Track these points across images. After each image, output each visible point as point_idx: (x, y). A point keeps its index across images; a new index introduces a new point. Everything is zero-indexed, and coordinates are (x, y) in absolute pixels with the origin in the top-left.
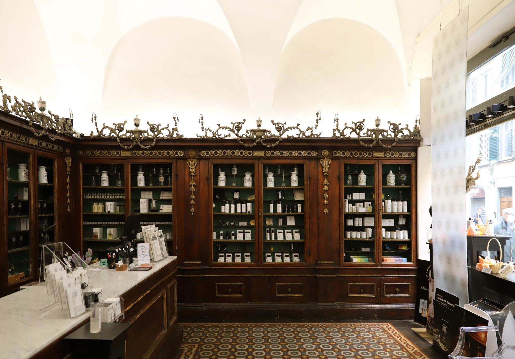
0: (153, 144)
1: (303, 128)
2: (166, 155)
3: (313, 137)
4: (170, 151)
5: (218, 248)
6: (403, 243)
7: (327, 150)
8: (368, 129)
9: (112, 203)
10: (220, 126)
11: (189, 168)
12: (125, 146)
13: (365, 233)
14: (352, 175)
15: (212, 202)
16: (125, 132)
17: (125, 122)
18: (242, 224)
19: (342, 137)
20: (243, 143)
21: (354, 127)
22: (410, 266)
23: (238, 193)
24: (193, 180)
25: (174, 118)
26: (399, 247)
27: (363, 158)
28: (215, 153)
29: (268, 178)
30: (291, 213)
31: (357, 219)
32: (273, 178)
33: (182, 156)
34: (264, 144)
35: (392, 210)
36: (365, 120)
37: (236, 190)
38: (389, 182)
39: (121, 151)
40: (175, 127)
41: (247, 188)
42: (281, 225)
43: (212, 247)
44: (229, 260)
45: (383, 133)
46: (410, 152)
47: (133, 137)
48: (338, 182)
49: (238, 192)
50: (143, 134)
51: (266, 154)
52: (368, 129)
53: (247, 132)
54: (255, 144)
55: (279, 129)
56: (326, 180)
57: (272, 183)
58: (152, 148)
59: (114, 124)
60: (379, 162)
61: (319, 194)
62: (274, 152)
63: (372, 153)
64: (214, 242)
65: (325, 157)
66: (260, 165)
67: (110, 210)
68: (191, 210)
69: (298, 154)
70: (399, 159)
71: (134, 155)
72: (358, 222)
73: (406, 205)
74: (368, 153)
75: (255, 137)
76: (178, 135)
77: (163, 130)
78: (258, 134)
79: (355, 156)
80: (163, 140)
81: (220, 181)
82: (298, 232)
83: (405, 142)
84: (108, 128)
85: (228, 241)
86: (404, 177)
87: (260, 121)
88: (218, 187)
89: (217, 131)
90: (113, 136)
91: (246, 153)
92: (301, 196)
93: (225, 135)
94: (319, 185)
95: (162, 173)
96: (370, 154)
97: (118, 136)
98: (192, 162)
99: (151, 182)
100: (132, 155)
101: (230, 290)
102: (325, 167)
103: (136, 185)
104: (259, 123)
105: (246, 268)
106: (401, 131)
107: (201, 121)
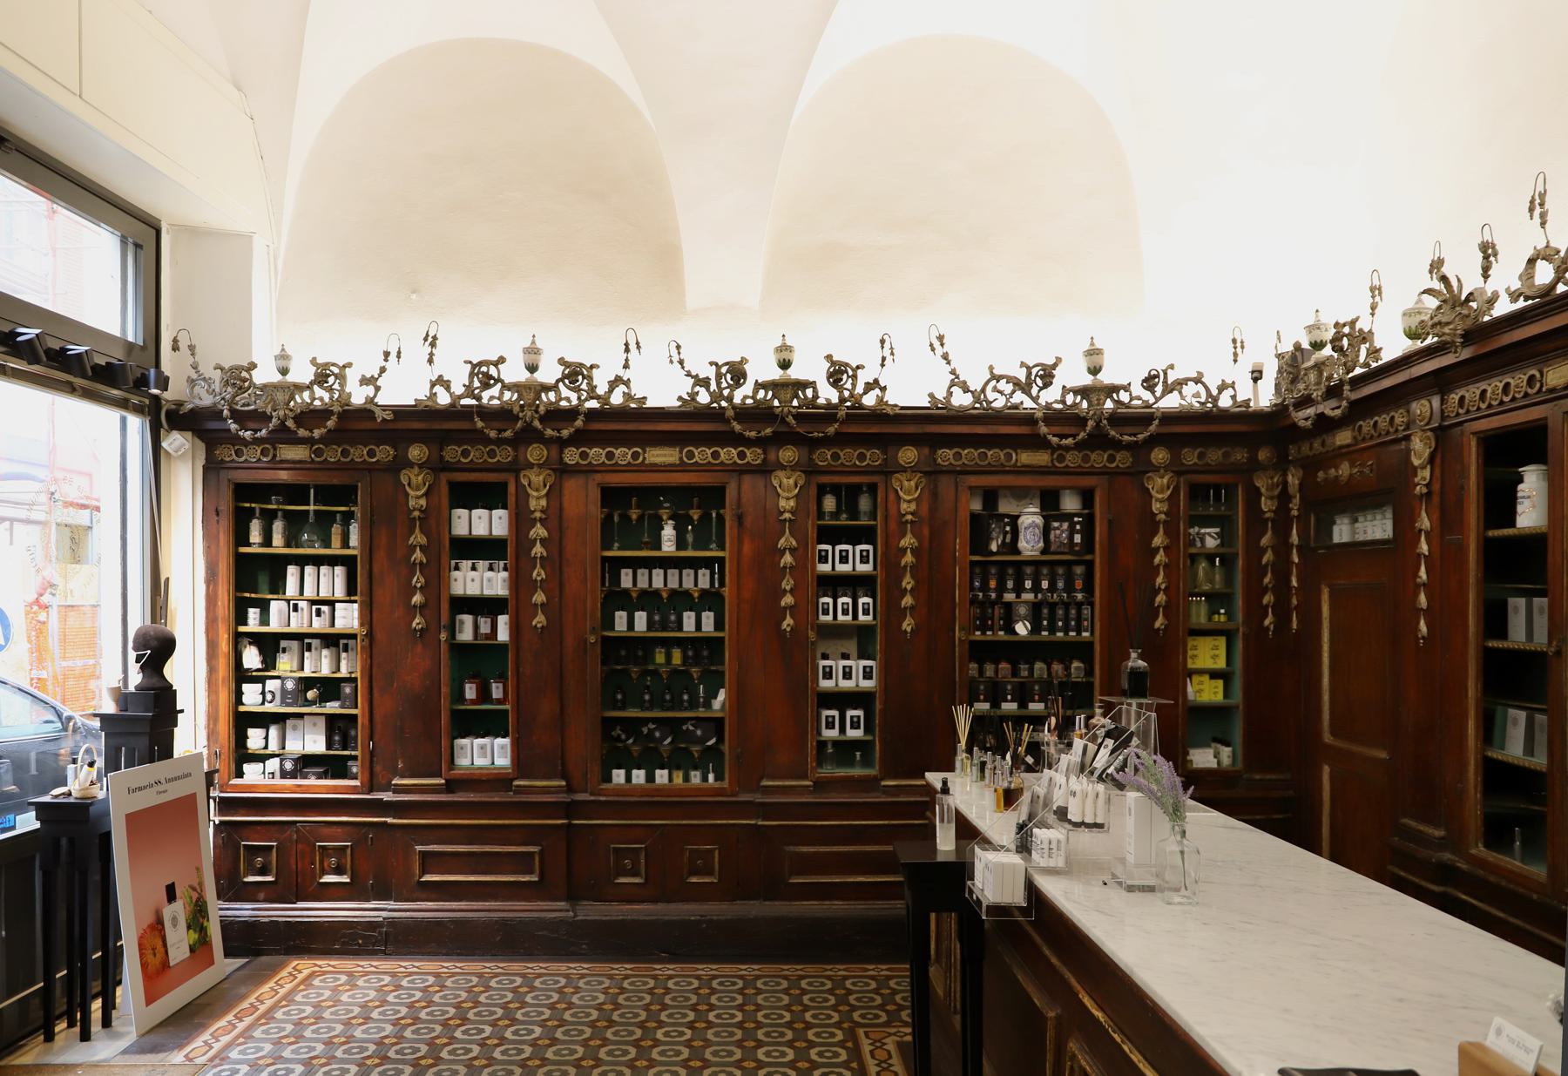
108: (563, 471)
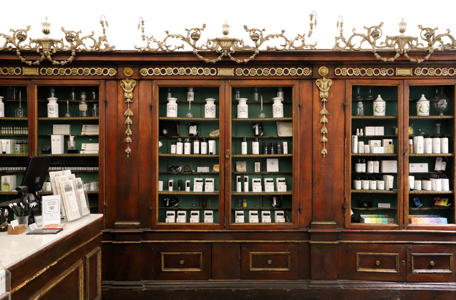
0: (70, 59)
1: (291, 36)
2: (90, 75)
3: (305, 48)
4: (96, 69)
5: (166, 204)
6: (442, 196)
7: (327, 67)
8: (387, 36)
9: (9, 141)
10: (169, 33)
11: (124, 91)
12: (29, 61)
13: (383, 182)
14: (364, 102)
15: (157, 139)
16: (29, 41)
17: (29, 28)
18: (200, 169)
19: (348, 48)
20: (202, 57)
21: (366, 34)
22: (452, 229)
23: (195, 127)
24: (129, 109)
25: (102, 23)
26: (436, 202)
27: (380, 78)
28: (161, 71)
29: (238, 106)
30: (272, 155)
31: (371, 163)
32: (247, 105)
33: (114, 75)
34: (233, 59)
35: (425, 150)
36: (383, 23)
37: (193, 123)
38: (420, 111)
39: (23, 68)
40: (102, 35)
41: (209, 119)
42: (259, 171)
43: (157, 202)
44: (182, 220)
45: (411, 42)
46: (453, 69)
47: (40, 49)
48: (342, 111)
49: (196, 126)
50: (55, 45)
51: (236, 73)
52: (387, 36)
53: (209, 42)
54: (219, 58)
55: (255, 38)
56: (324, 108)
57: (245, 113)
58: (69, 65)
59: (11, 30)
60: (405, 83)
61: (315, 128)
62: (248, 70)
63: (393, 71)
64: (160, 195)
65: (323, 76)
66: (227, 88)
67: (6, 150)
68: (126, 151)
69: (283, 72)
70: (435, 78)
71: (42, 74)
72: (373, 167)
73: (446, 143)
74: (388, 70)
75: (220, 49)
76: (107, 46)
77: (85, 39)
78: (224, 44)
79: (368, 75)
80: (84, 53)
81: (169, 110)
82: (284, 181)
83: (444, 53)
84: (2, 36)
85: (181, 193)
86: (443, 104)
87: (227, 27)
88: (166, 118)
89: (165, 40)
90: (10, 47)
91: (207, 72)
92: (287, 131)
93: (176, 47)
94: (314, 116)
95: (84, 100)
96: (390, 72)
97: (18, 47)
98: (127, 83)
99: (68, 112)
100: (40, 74)
101: (182, 262)
102: (323, 90)
103: (46, 115)
104: (226, 29)
105: (206, 231)
106: (439, 39)
107: (141, 26)
108: (140, 79)
